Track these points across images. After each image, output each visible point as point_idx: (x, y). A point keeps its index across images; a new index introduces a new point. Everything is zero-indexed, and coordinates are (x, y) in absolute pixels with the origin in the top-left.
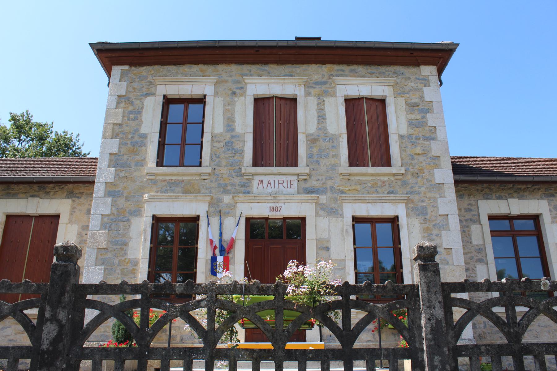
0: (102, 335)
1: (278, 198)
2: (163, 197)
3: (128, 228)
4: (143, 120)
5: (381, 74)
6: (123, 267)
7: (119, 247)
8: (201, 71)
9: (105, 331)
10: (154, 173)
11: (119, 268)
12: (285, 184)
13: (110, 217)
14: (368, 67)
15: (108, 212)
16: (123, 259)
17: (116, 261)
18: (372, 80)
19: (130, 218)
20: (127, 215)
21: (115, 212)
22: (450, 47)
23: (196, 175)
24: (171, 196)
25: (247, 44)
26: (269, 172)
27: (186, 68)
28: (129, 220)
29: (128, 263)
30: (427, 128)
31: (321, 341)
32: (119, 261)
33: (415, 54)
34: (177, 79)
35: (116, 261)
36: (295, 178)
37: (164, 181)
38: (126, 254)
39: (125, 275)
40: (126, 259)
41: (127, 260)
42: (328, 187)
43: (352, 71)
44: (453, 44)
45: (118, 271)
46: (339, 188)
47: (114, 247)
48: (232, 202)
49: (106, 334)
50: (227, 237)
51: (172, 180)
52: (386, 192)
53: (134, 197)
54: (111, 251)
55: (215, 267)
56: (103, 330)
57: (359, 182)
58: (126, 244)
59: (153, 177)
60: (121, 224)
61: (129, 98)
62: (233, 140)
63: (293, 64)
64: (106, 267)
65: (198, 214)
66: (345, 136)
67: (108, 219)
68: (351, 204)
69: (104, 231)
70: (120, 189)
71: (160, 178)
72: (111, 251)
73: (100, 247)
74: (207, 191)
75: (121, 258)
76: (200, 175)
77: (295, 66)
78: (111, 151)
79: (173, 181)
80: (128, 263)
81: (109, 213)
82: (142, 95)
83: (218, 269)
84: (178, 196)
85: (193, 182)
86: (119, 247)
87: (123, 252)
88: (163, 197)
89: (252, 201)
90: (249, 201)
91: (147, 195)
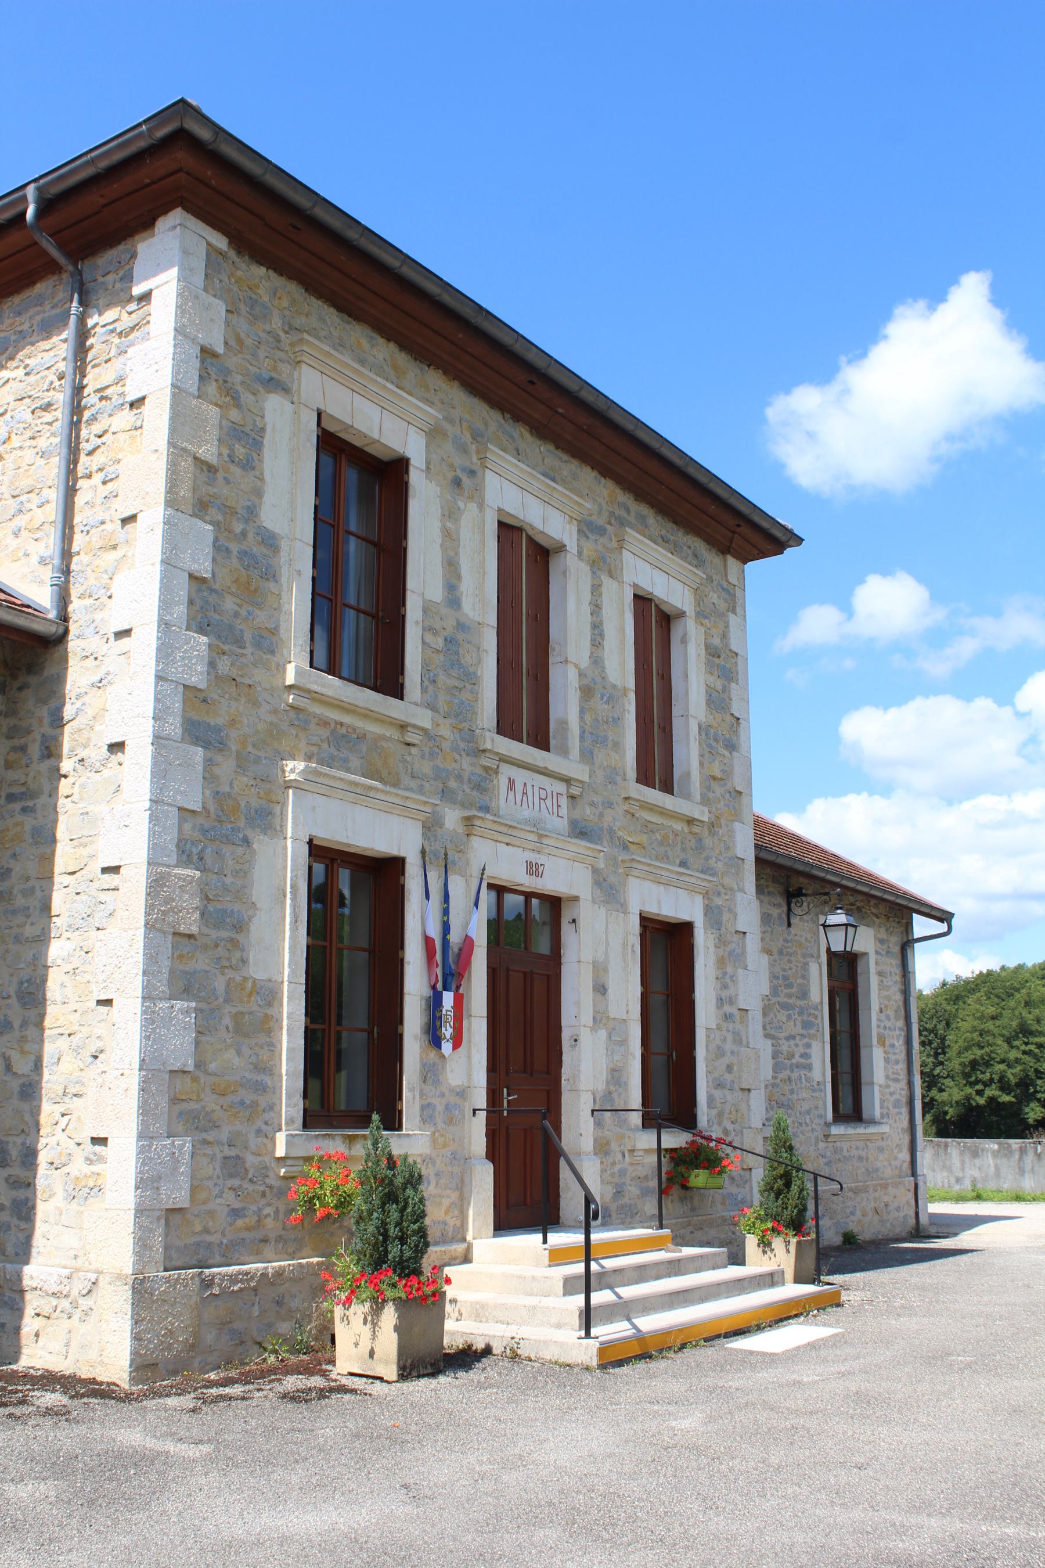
0: (198, 1244)
1: (545, 841)
2: (337, 784)
3: (244, 872)
4: (267, 476)
5: (676, 550)
6: (241, 1009)
7: (225, 934)
8: (395, 367)
9: (206, 1231)
10: (309, 691)
11: (228, 1009)
12: (549, 802)
13: (200, 820)
14: (670, 526)
15: (195, 804)
16: (238, 979)
17: (220, 984)
18: (674, 563)
19: (249, 833)
20: (242, 823)
21: (212, 807)
22: (778, 534)
23: (391, 724)
24: (357, 784)
25: (531, 356)
26: (541, 764)
27: (358, 334)
28: (247, 842)
29: (250, 995)
30: (728, 718)
31: (661, 1227)
32: (228, 984)
33: (744, 529)
34: (356, 371)
35: (220, 984)
36: (560, 787)
37: (324, 723)
38: (244, 961)
39: (246, 1036)
40: (245, 979)
41: (249, 985)
42: (605, 825)
43: (642, 518)
44: (791, 532)
45: (227, 1021)
46: (620, 833)
47: (214, 933)
48: (461, 830)
49: (209, 1238)
50: (455, 938)
51: (342, 724)
52: (678, 862)
53: (257, 760)
54: (206, 947)
55: (438, 1024)
56: (198, 1228)
57: (648, 828)
58: (240, 926)
59: (303, 703)
60: (227, 850)
61: (229, 372)
62: (460, 636)
63: (557, 448)
64: (202, 1005)
65: (402, 854)
66: (632, 696)
67: (193, 828)
68: (638, 880)
69: (189, 872)
70: (220, 721)
71: (318, 710)
72: (206, 947)
73: (182, 929)
74: (413, 784)
75: (230, 973)
76: (403, 727)
77: (559, 453)
78: (194, 567)
79: (344, 731)
80: (250, 995)
81: (197, 806)
82: (259, 379)
83: (443, 1029)
84: (371, 788)
85: (383, 743)
86: (225, 934)
87: (238, 954)
88: (337, 784)
89: (501, 838)
90: (497, 836)
91: (301, 765)
